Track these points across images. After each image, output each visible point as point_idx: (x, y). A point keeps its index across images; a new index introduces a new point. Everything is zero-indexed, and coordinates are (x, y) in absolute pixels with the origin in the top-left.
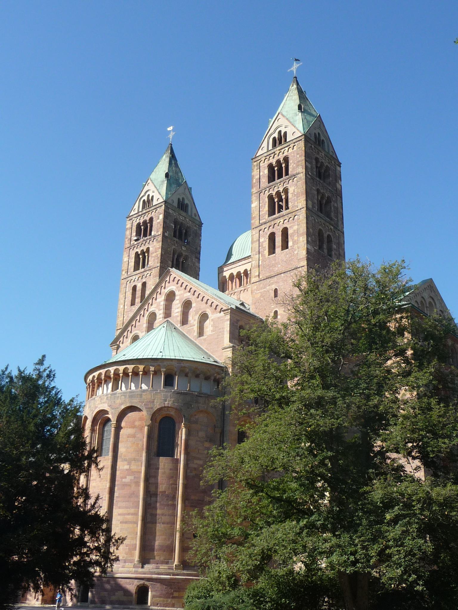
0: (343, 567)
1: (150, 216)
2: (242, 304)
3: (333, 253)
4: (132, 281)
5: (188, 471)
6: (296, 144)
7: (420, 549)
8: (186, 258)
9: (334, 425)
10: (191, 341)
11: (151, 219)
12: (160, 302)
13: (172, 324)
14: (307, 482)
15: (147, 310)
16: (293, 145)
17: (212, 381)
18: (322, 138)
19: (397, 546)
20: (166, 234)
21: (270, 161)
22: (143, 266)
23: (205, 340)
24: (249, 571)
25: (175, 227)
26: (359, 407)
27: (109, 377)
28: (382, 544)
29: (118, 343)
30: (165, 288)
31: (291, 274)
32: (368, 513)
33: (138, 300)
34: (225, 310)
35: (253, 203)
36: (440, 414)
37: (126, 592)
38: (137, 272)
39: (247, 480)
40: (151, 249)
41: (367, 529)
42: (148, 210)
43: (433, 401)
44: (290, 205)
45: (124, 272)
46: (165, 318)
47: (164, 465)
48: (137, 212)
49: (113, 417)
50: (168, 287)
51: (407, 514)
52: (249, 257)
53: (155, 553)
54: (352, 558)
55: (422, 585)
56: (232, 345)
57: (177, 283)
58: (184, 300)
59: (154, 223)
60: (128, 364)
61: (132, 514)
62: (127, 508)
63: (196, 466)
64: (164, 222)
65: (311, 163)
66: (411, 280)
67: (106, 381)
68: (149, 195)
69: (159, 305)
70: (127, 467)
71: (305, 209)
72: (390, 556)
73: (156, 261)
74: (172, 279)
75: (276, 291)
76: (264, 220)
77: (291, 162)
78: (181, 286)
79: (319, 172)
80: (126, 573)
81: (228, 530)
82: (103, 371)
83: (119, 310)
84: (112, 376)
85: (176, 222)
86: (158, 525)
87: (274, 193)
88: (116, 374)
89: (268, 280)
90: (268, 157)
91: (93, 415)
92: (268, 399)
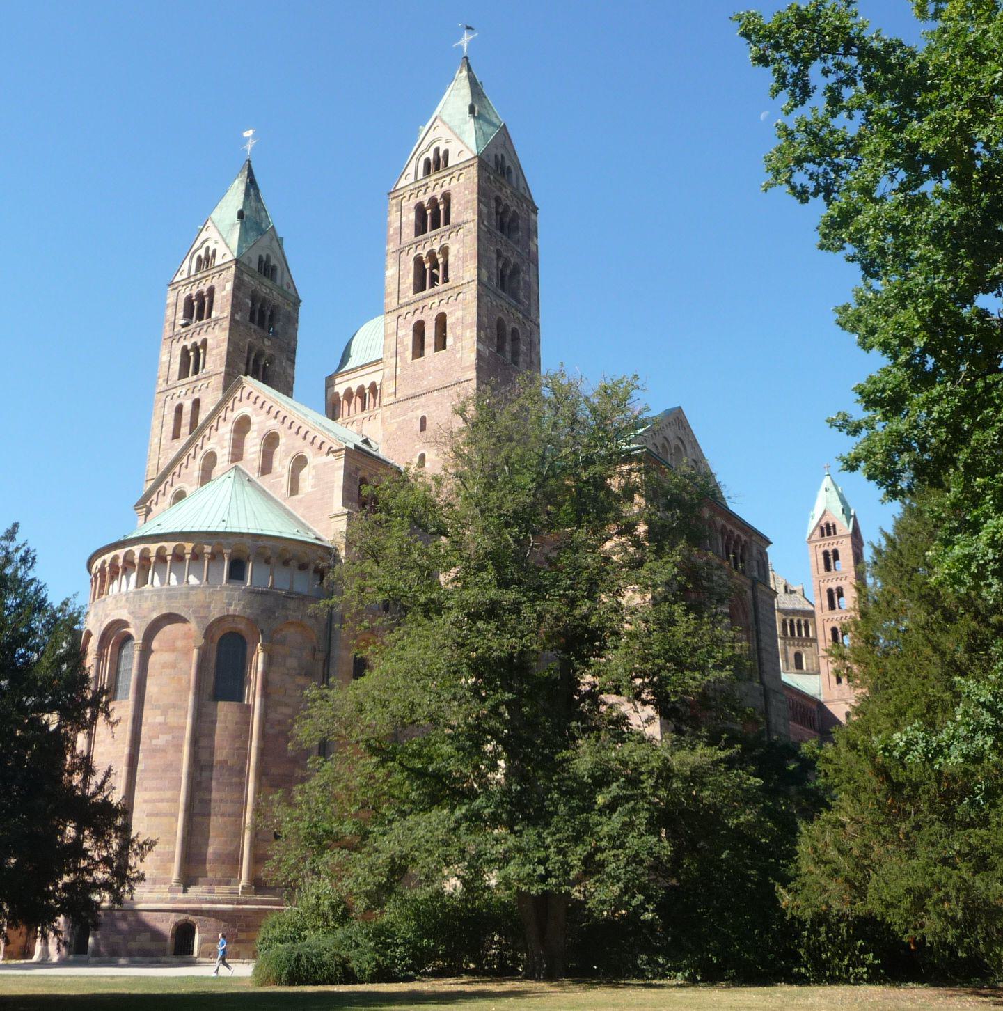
0: (525, 884)
1: (209, 284)
2: (366, 441)
3: (521, 359)
4: (175, 396)
5: (268, 725)
7: (650, 853)
8: (271, 360)
9: (515, 648)
10: (276, 502)
11: (211, 290)
12: (223, 435)
13: (243, 473)
14: (468, 743)
15: (202, 448)
16: (459, 172)
17: (311, 572)
18: (508, 163)
19: (613, 848)
20: (237, 317)
22: (196, 371)
23: (300, 501)
24: (368, 894)
25: (253, 305)
26: (557, 619)
27: (132, 564)
28: (590, 844)
29: (148, 504)
30: (232, 410)
32: (568, 794)
33: (185, 430)
34: (336, 451)
36: (688, 631)
37: (156, 935)
38: (185, 381)
39: (367, 740)
40: (209, 342)
41: (565, 821)
42: (206, 274)
43: (678, 610)
44: (451, 274)
45: (161, 381)
46: (232, 461)
47: (226, 716)
48: (185, 276)
49: (137, 633)
50: (238, 409)
51: (632, 796)
52: (379, 361)
53: (208, 866)
54: (541, 870)
55: (653, 911)
56: (346, 510)
57: (255, 403)
58: (265, 432)
59: (217, 297)
60: (166, 541)
61: (168, 801)
62: (158, 789)
63: (279, 717)
64: (235, 296)
65: (488, 205)
66: (647, 409)
67: (125, 570)
68: (208, 249)
69: (221, 440)
70: (160, 719)
71: (476, 282)
72: (602, 864)
73: (219, 362)
74: (245, 394)
75: (423, 420)
76: (406, 300)
77: (454, 202)
78: (262, 407)
79: (501, 219)
80: (156, 902)
81: (335, 825)
82: (120, 553)
84: (137, 561)
85: (254, 297)
86: (213, 818)
87: (424, 254)
88: (144, 557)
89: (410, 402)
90: (416, 192)
91: (102, 628)
92: (406, 604)
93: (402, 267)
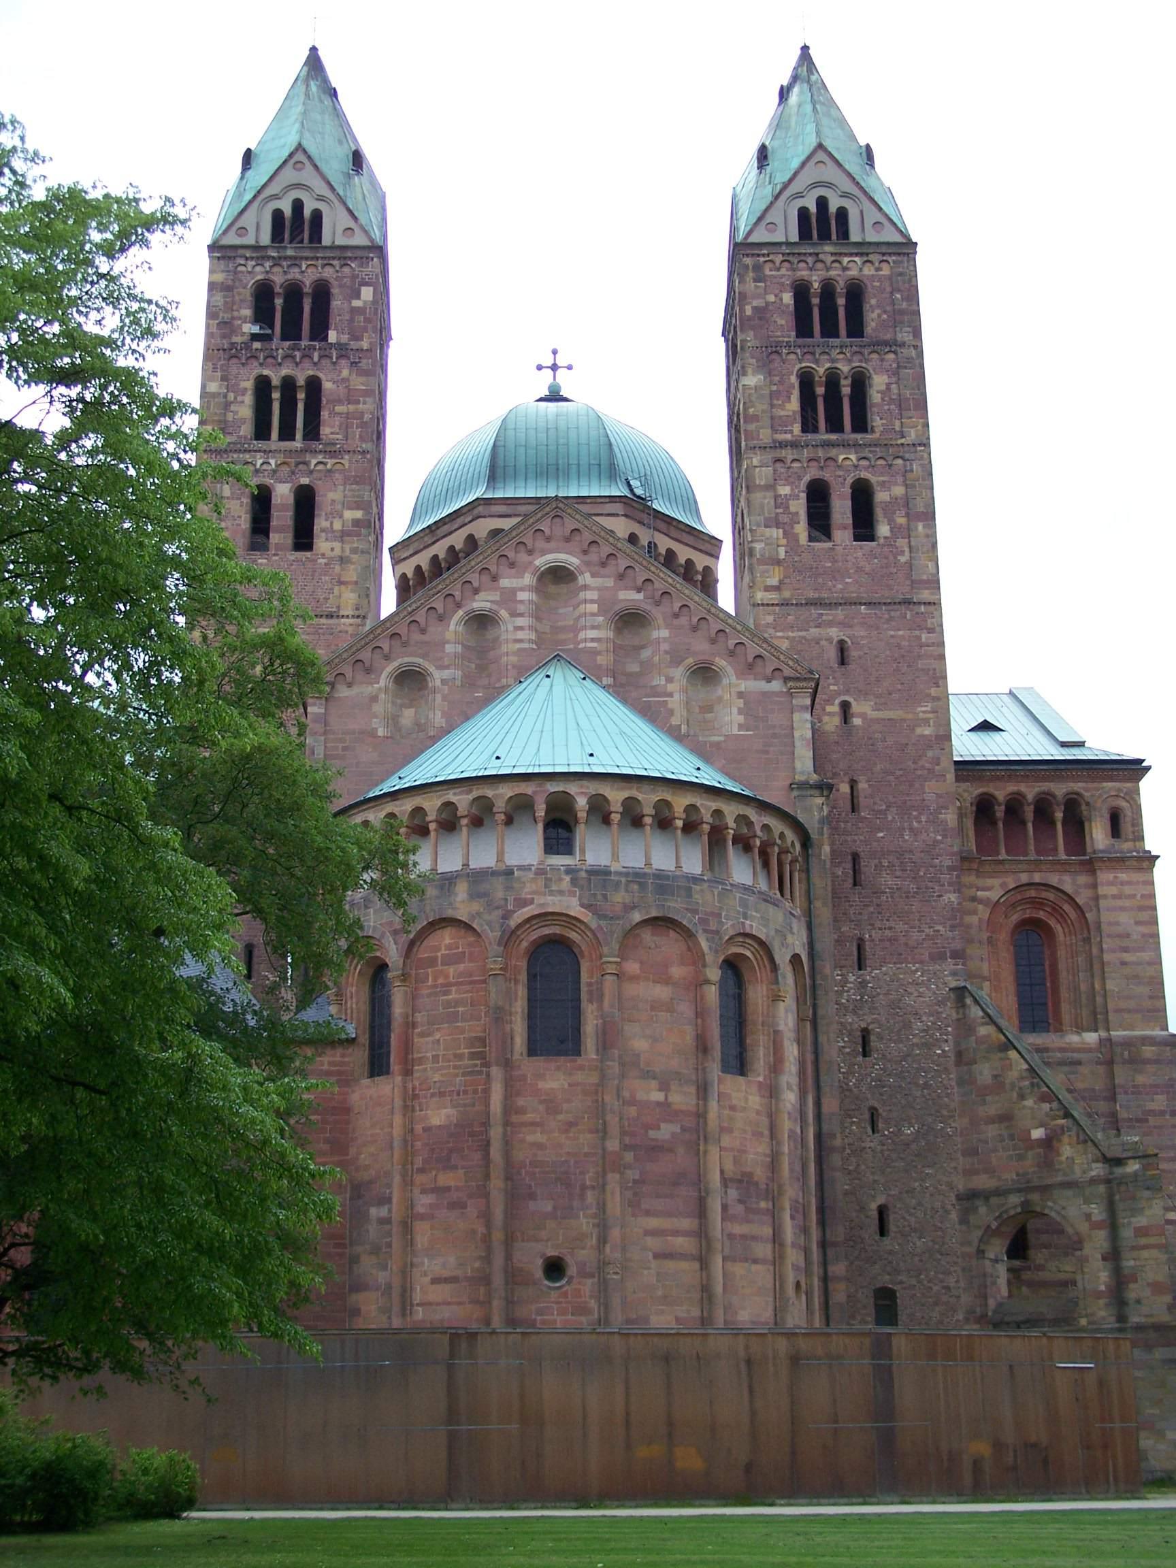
6: (890, 259)
12: (514, 591)
21: (804, 274)
30: (530, 552)
31: (893, 614)
35: (745, 374)
40: (327, 385)
42: (307, 254)
58: (617, 608)
61: (686, 1234)
62: (669, 1214)
67: (509, 821)
68: (298, 206)
75: (842, 648)
76: (788, 437)
91: (513, 922)
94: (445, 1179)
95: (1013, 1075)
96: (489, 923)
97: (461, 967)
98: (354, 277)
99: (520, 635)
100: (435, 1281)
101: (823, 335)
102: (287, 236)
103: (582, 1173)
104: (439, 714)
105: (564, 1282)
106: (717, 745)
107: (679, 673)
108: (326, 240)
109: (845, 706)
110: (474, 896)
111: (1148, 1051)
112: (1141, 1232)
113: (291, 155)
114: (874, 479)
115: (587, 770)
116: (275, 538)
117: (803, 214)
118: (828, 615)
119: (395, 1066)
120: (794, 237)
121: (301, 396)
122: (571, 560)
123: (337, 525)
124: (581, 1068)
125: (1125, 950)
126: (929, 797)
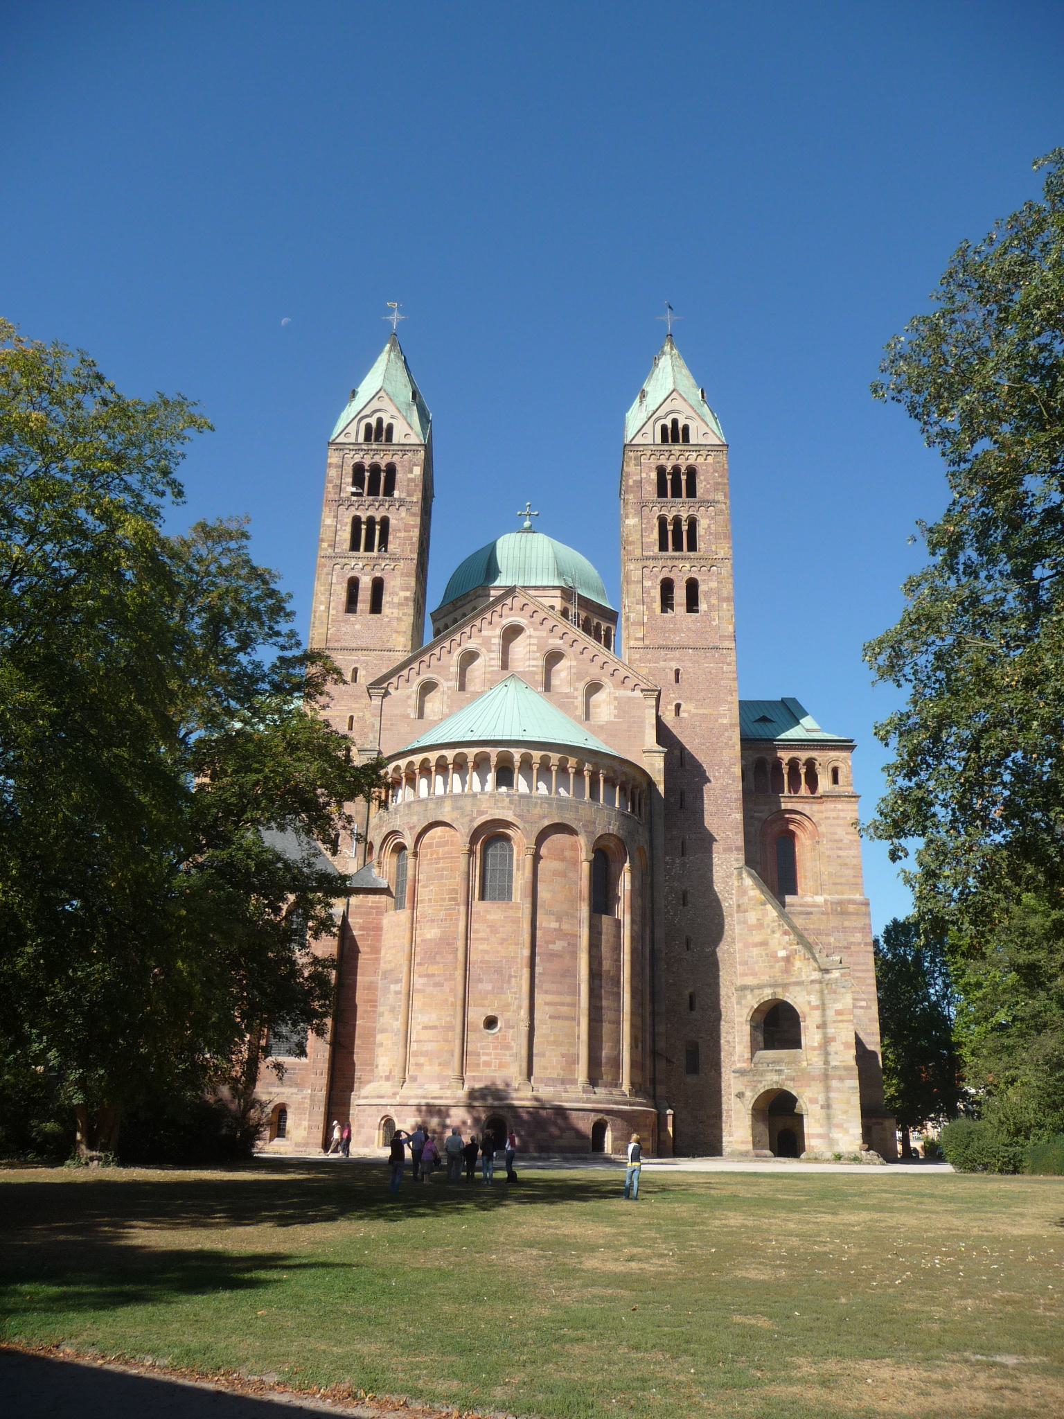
4: (348, 567)
6: (712, 454)
12: (490, 638)
15: (460, 645)
21: (663, 461)
29: (385, 685)
37: (579, 1134)
40: (392, 522)
45: (325, 545)
50: (508, 616)
58: (549, 648)
61: (569, 1005)
62: (559, 993)
68: (380, 421)
70: (554, 925)
75: (677, 672)
76: (651, 553)
78: (542, 624)
83: (315, 612)
87: (670, 518)
90: (658, 454)
91: (476, 824)
93: (645, 521)
94: (433, 969)
95: (768, 920)
96: (462, 824)
97: (446, 848)
98: (411, 461)
99: (493, 663)
100: (425, 1028)
101: (673, 497)
102: (373, 438)
103: (510, 968)
104: (445, 707)
105: (496, 1030)
106: (601, 727)
107: (582, 686)
108: (395, 440)
109: (678, 707)
110: (455, 808)
111: (851, 908)
112: (838, 1013)
113: (377, 393)
114: (699, 578)
115: (521, 739)
116: (360, 606)
117: (664, 428)
118: (671, 654)
119: (407, 905)
120: (658, 440)
121: (378, 527)
122: (522, 621)
123: (396, 600)
124: (511, 908)
125: (840, 849)
126: (725, 758)
